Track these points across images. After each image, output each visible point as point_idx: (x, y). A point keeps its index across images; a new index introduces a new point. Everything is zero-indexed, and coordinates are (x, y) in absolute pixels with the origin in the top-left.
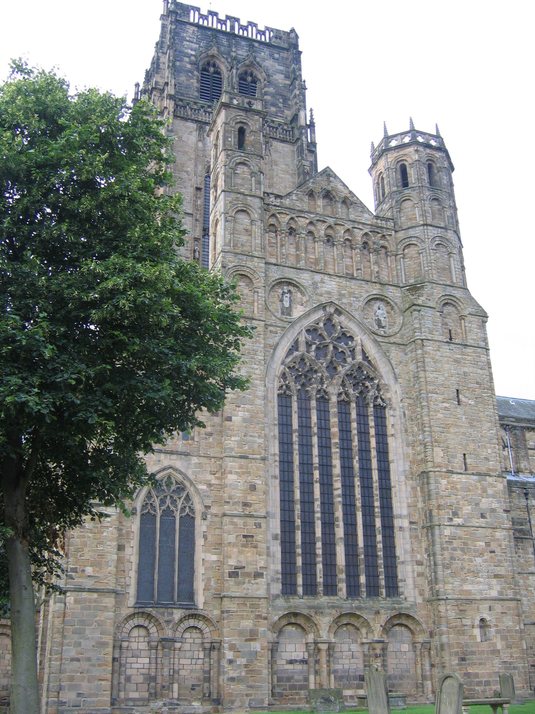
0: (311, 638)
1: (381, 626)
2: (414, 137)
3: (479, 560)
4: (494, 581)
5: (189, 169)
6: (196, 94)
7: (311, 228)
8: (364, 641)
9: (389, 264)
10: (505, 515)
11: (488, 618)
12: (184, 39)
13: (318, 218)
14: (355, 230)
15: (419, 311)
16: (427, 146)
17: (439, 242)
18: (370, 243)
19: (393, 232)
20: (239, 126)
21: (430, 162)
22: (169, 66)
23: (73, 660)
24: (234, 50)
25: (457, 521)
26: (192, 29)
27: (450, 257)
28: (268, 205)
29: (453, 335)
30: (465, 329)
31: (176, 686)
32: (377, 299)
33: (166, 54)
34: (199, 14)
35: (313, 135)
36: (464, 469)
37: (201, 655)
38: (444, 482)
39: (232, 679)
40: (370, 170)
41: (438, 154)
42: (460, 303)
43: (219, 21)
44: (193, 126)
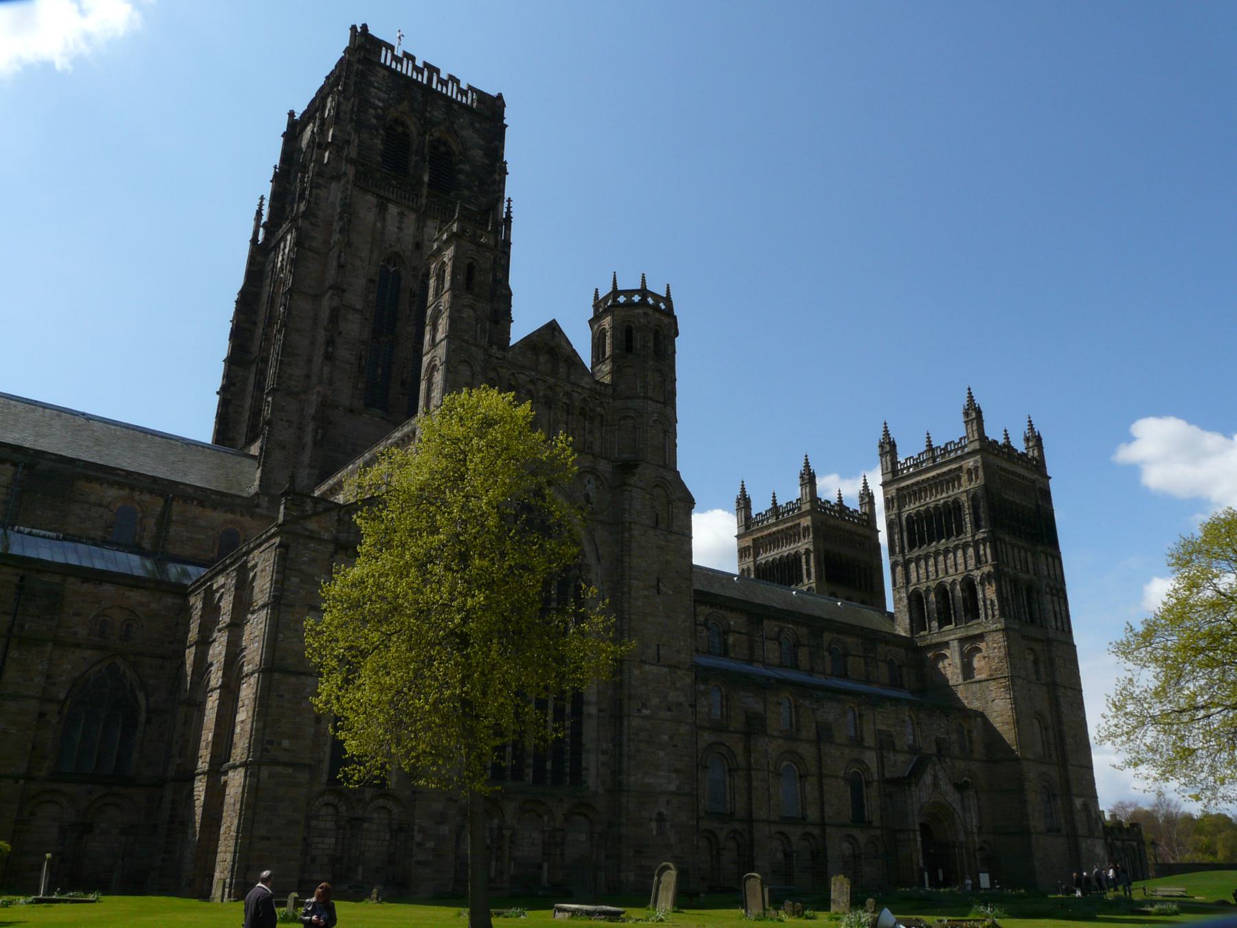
0: (496, 821)
1: (563, 814)
2: (644, 298)
3: (662, 754)
4: (674, 776)
5: (363, 255)
6: (379, 159)
7: (531, 387)
8: (546, 828)
9: (603, 434)
10: (690, 710)
11: (665, 812)
12: (371, 84)
13: (538, 377)
14: (574, 393)
15: (630, 491)
16: (656, 308)
17: (657, 418)
18: (587, 409)
19: (611, 400)
20: (469, 261)
21: (657, 328)
22: (351, 120)
23: (262, 838)
24: (429, 109)
25: (646, 712)
26: (383, 72)
27: (665, 435)
28: (490, 356)
29: (660, 519)
30: (672, 515)
31: (360, 869)
32: (588, 472)
33: (349, 100)
34: (393, 54)
35: (508, 232)
36: (657, 660)
37: (388, 837)
38: (636, 672)
39: (419, 863)
40: (591, 322)
41: (666, 320)
42: (670, 487)
43: (415, 68)
44: (371, 199)
